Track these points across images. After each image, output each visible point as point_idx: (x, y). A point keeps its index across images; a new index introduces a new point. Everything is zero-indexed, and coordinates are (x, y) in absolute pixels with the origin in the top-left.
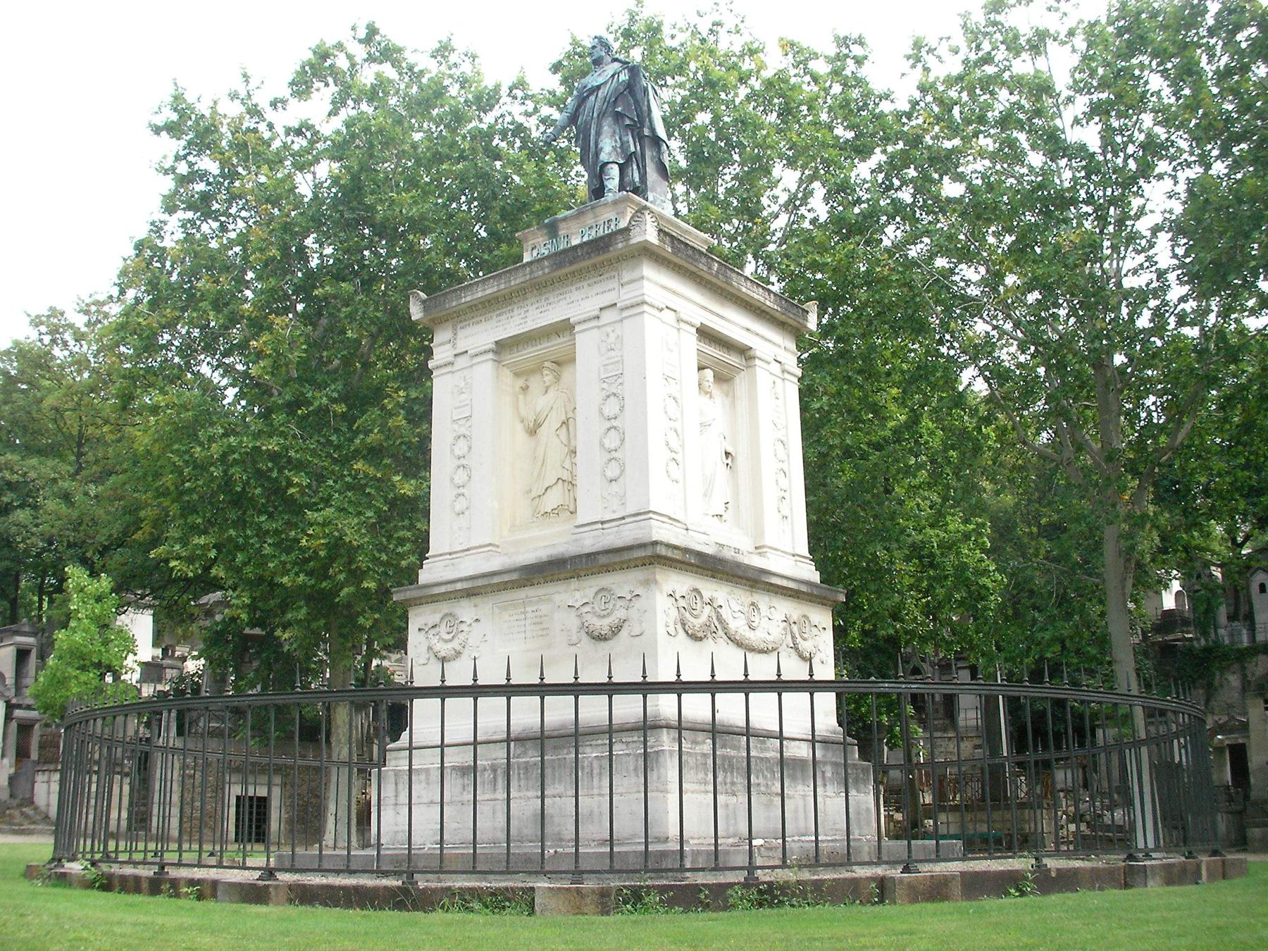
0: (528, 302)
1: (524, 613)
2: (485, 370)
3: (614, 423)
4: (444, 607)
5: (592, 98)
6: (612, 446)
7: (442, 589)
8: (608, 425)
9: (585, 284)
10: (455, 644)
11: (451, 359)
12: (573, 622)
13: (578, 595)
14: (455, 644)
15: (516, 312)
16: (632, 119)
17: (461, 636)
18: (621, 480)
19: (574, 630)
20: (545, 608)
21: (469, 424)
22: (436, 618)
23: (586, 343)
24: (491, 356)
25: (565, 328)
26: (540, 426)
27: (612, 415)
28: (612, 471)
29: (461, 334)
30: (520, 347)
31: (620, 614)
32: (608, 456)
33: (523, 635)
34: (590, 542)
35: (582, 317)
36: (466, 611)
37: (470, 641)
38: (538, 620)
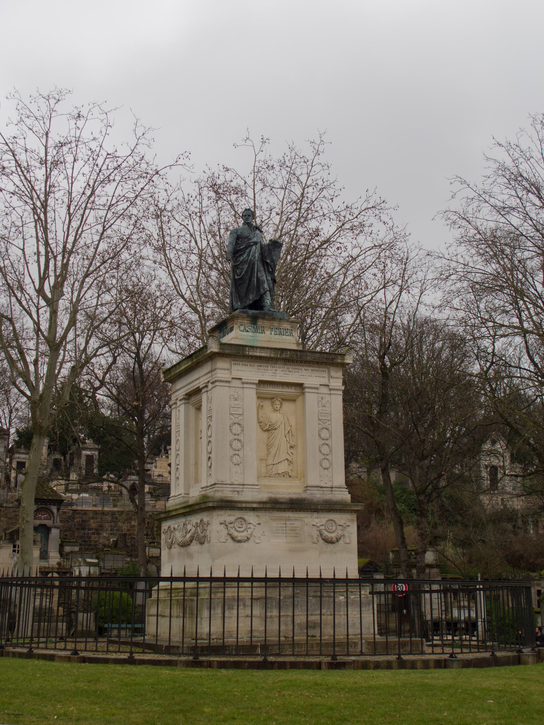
0: (277, 366)
2: (251, 394)
3: (327, 442)
4: (238, 514)
5: (254, 247)
6: (326, 453)
7: (244, 505)
9: (310, 369)
10: (245, 534)
11: (230, 379)
12: (315, 533)
13: (317, 520)
14: (245, 534)
15: (269, 368)
18: (330, 470)
19: (315, 536)
20: (297, 524)
21: (241, 418)
22: (232, 519)
23: (310, 398)
24: (254, 386)
26: (275, 429)
28: (326, 464)
29: (234, 367)
31: (340, 533)
32: (323, 457)
34: (318, 496)
36: (251, 517)
37: (254, 534)
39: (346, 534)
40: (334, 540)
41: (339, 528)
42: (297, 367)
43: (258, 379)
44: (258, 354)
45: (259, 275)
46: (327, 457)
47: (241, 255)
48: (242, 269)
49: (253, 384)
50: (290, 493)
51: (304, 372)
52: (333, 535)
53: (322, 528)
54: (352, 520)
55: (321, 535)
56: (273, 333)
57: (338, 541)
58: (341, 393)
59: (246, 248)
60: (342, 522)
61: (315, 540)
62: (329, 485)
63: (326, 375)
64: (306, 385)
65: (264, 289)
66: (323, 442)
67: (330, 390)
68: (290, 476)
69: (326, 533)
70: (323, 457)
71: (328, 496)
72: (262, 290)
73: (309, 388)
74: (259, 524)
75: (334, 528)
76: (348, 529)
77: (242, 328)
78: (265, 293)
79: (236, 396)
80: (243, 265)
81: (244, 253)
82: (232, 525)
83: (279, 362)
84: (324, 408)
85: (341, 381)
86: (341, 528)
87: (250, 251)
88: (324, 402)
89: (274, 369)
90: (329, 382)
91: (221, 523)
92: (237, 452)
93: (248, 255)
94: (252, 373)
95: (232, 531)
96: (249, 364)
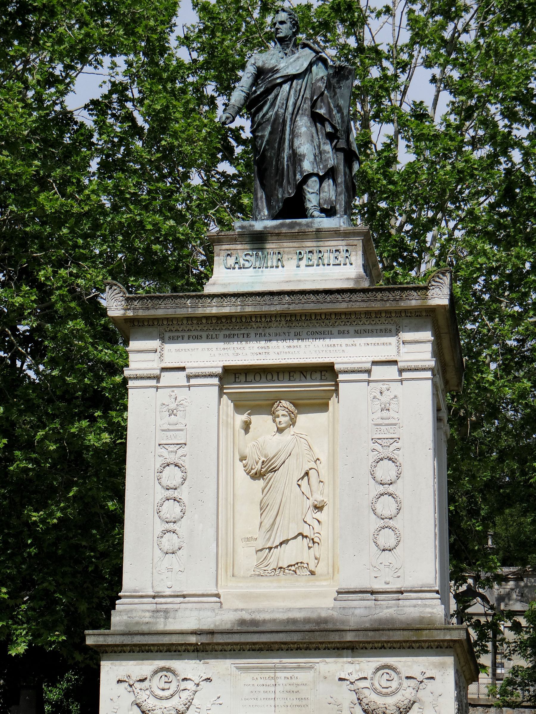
1: (275, 678)
3: (391, 489)
5: (286, 87)
8: (381, 489)
9: (352, 329)
13: (350, 668)
16: (333, 127)
17: (185, 695)
19: (346, 705)
20: (302, 676)
25: (327, 371)
26: (274, 470)
27: (387, 480)
28: (387, 538)
30: (250, 377)
32: (381, 523)
33: (272, 702)
34: (360, 611)
35: (349, 367)
36: (189, 667)
38: (294, 688)
41: (406, 683)
43: (222, 364)
44: (214, 311)
45: (297, 143)
46: (391, 523)
47: (260, 109)
48: (262, 137)
49: (211, 376)
50: (289, 610)
53: (362, 684)
54: (443, 666)
56: (303, 263)
58: (429, 374)
59: (268, 91)
60: (415, 671)
64: (336, 367)
66: (381, 489)
68: (312, 573)
70: (381, 523)
71: (387, 610)
73: (346, 372)
74: (208, 680)
75: (394, 685)
77: (231, 261)
79: (173, 406)
80: (264, 129)
83: (274, 324)
84: (385, 414)
86: (412, 683)
87: (278, 95)
88: (384, 399)
91: (119, 681)
92: (171, 526)
93: (273, 104)
95: (143, 696)
96: (204, 334)
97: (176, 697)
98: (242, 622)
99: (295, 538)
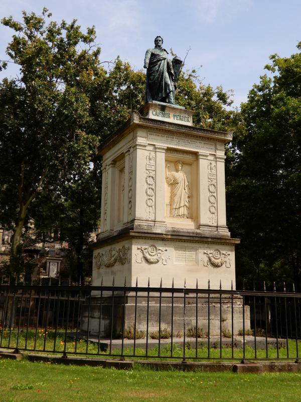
2: (161, 156)
3: (214, 195)
5: (163, 61)
10: (155, 257)
14: (155, 257)
26: (178, 183)
39: (228, 261)
40: (220, 264)
42: (194, 140)
51: (199, 144)
52: (216, 261)
53: (211, 255)
54: (232, 251)
55: (210, 260)
57: (222, 265)
59: (158, 61)
61: (206, 264)
62: (215, 224)
63: (213, 147)
65: (169, 90)
67: (216, 158)
69: (213, 259)
70: (211, 205)
72: (168, 91)
74: (166, 250)
76: (229, 257)
77: (154, 113)
78: (170, 93)
81: (156, 65)
82: (146, 251)
85: (224, 152)
86: (224, 256)
89: (178, 140)
90: (216, 153)
92: (150, 197)
93: (159, 67)
94: (163, 143)
96: (160, 135)
97: (156, 256)
98: (174, 231)
99: (183, 206)
